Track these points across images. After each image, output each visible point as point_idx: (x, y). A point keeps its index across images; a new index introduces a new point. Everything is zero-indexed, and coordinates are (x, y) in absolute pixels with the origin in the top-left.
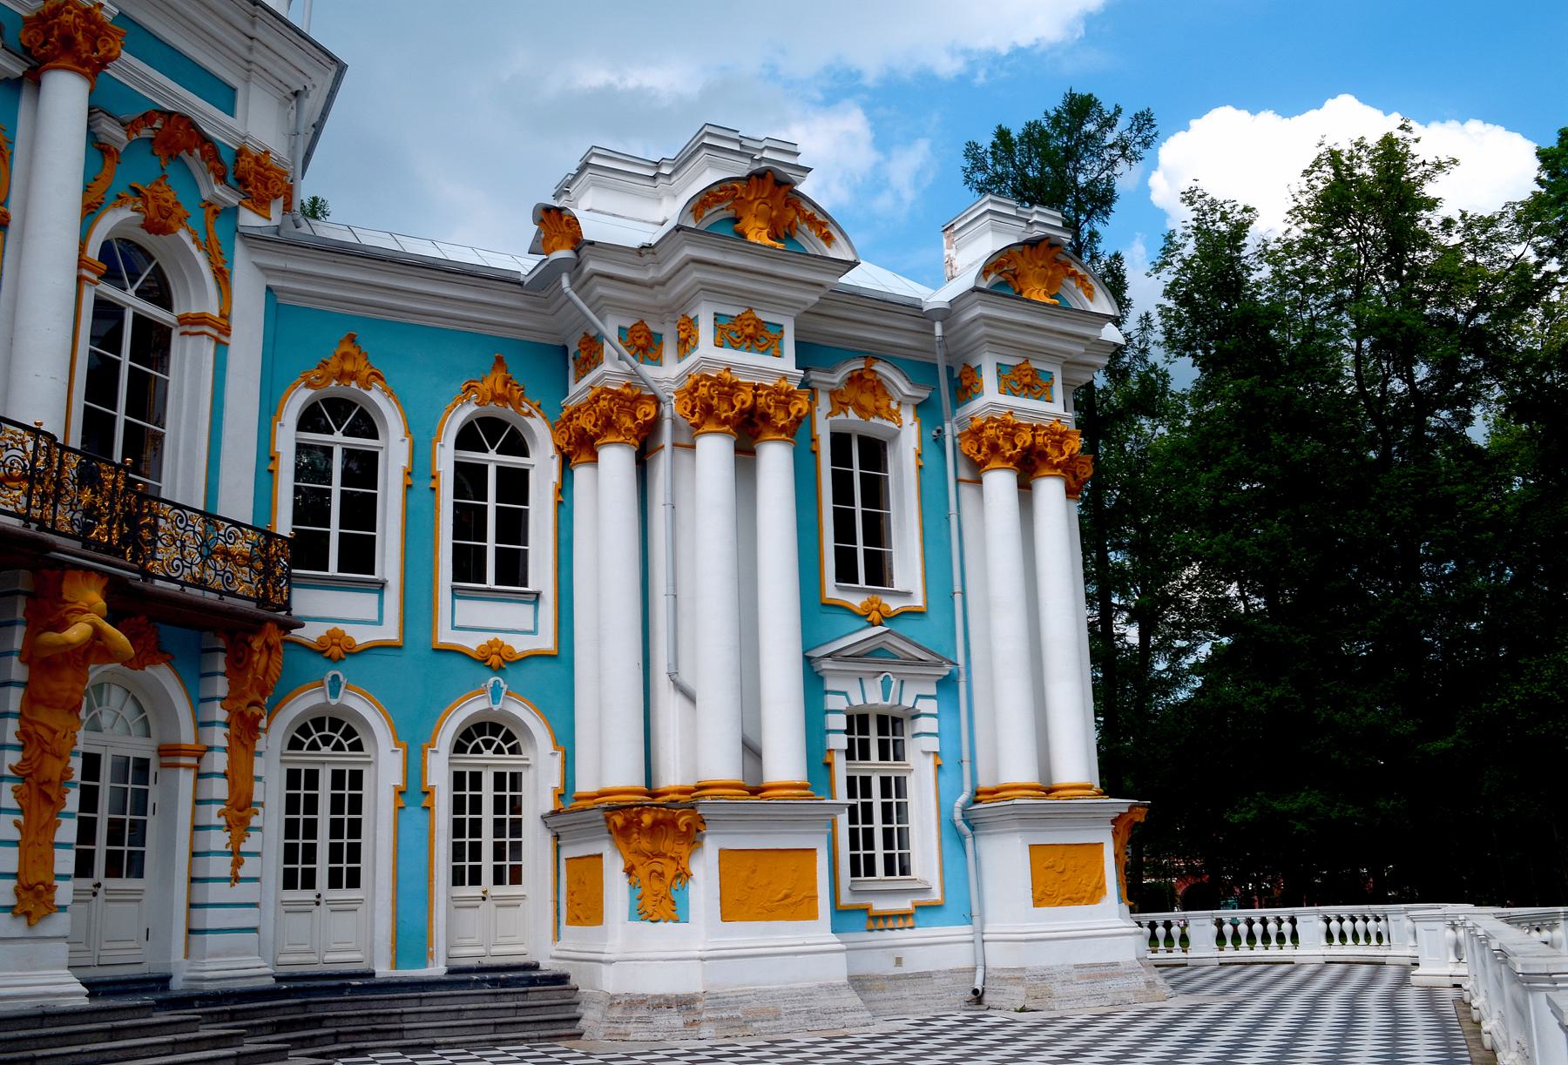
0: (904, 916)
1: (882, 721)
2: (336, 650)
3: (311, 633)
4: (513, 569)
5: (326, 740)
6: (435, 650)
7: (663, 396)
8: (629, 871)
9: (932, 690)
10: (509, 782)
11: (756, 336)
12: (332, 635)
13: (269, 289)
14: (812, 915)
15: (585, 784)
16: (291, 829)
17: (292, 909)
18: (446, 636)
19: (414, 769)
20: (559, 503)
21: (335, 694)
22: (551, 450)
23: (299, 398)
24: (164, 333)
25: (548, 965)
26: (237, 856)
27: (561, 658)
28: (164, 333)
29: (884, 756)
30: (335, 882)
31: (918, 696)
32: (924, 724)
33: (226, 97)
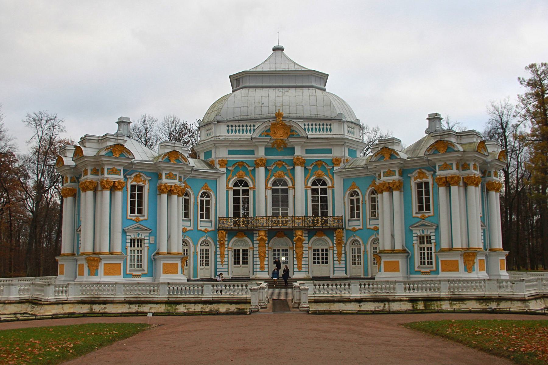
0: (429, 273)
1: (427, 237)
2: (354, 230)
3: (351, 228)
6: (368, 229)
9: (434, 231)
11: (390, 173)
12: (353, 228)
14: (399, 271)
17: (353, 268)
18: (369, 227)
19: (365, 248)
24: (326, 189)
26: (339, 260)
28: (326, 189)
29: (427, 243)
31: (431, 232)
33: (329, 151)
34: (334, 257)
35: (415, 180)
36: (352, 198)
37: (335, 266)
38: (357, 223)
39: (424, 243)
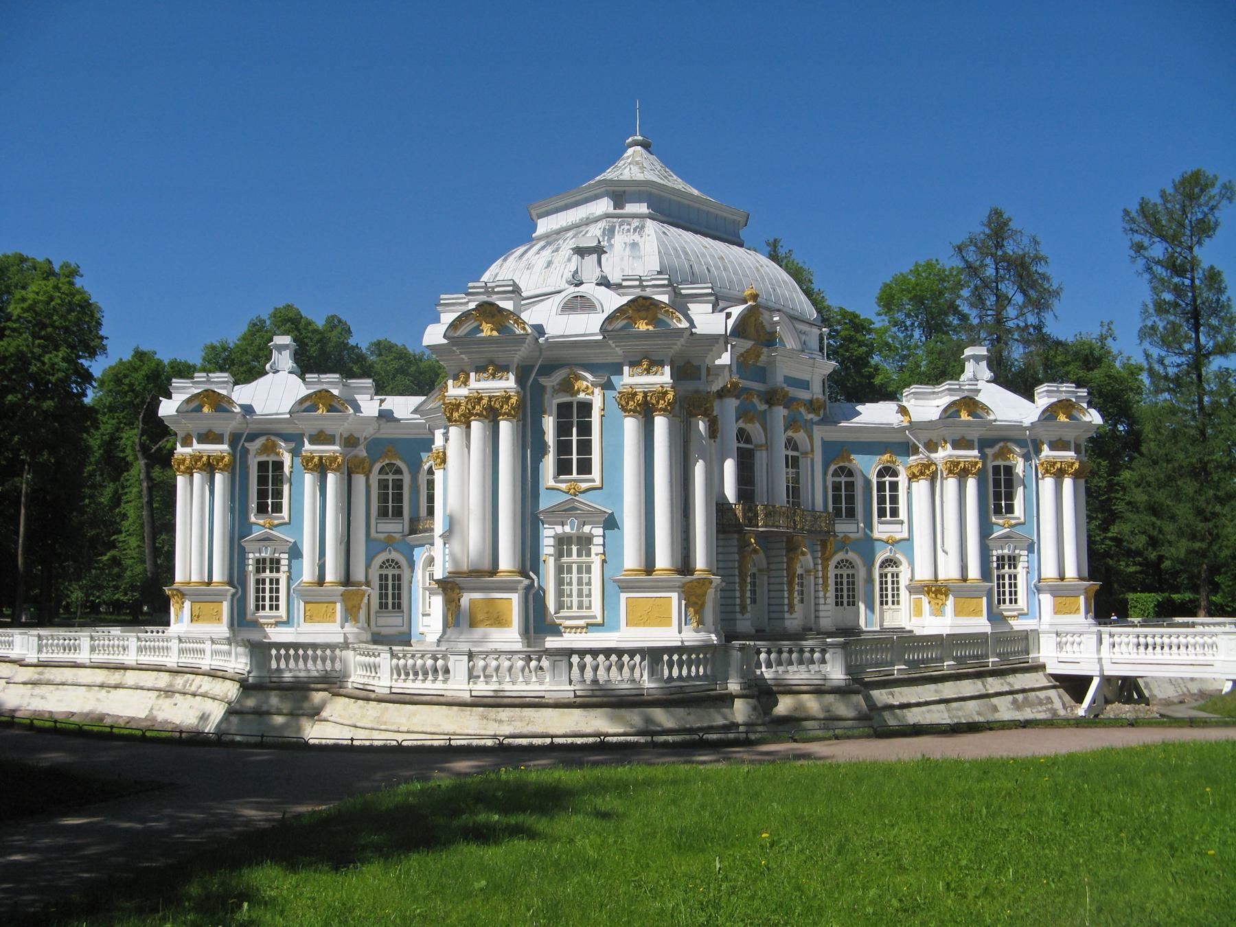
4: (895, 513)
5: (845, 565)
7: (938, 463)
8: (929, 603)
10: (896, 575)
13: (822, 438)
15: (917, 577)
16: (837, 590)
20: (908, 493)
21: (847, 553)
22: (905, 476)
23: (832, 468)
25: (908, 628)
26: (825, 598)
27: (909, 540)
30: (849, 605)
32: (1022, 558)
34: (816, 591)
35: (994, 461)
36: (837, 479)
37: (822, 607)
38: (852, 527)
39: (1003, 568)
